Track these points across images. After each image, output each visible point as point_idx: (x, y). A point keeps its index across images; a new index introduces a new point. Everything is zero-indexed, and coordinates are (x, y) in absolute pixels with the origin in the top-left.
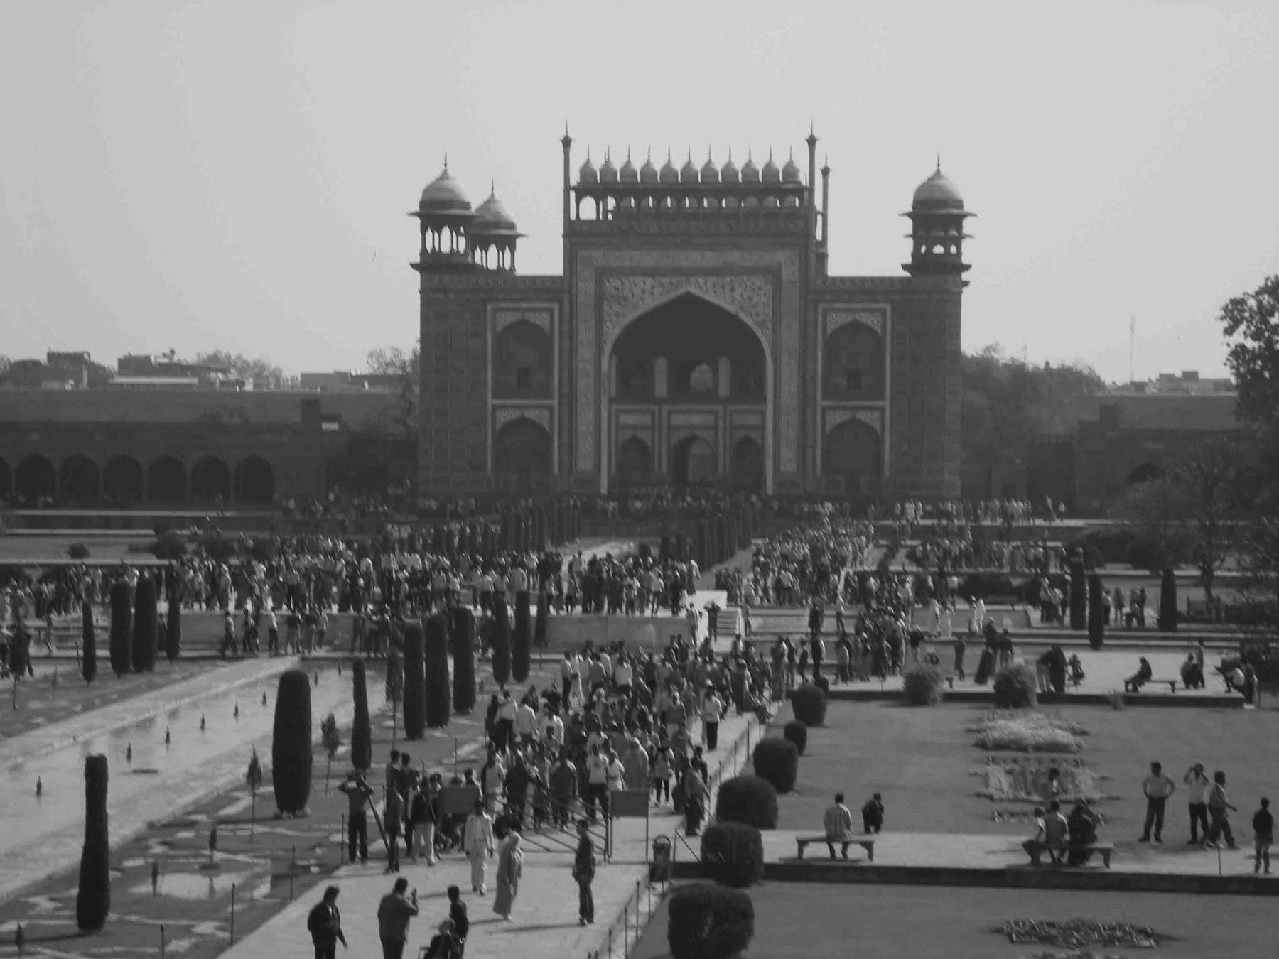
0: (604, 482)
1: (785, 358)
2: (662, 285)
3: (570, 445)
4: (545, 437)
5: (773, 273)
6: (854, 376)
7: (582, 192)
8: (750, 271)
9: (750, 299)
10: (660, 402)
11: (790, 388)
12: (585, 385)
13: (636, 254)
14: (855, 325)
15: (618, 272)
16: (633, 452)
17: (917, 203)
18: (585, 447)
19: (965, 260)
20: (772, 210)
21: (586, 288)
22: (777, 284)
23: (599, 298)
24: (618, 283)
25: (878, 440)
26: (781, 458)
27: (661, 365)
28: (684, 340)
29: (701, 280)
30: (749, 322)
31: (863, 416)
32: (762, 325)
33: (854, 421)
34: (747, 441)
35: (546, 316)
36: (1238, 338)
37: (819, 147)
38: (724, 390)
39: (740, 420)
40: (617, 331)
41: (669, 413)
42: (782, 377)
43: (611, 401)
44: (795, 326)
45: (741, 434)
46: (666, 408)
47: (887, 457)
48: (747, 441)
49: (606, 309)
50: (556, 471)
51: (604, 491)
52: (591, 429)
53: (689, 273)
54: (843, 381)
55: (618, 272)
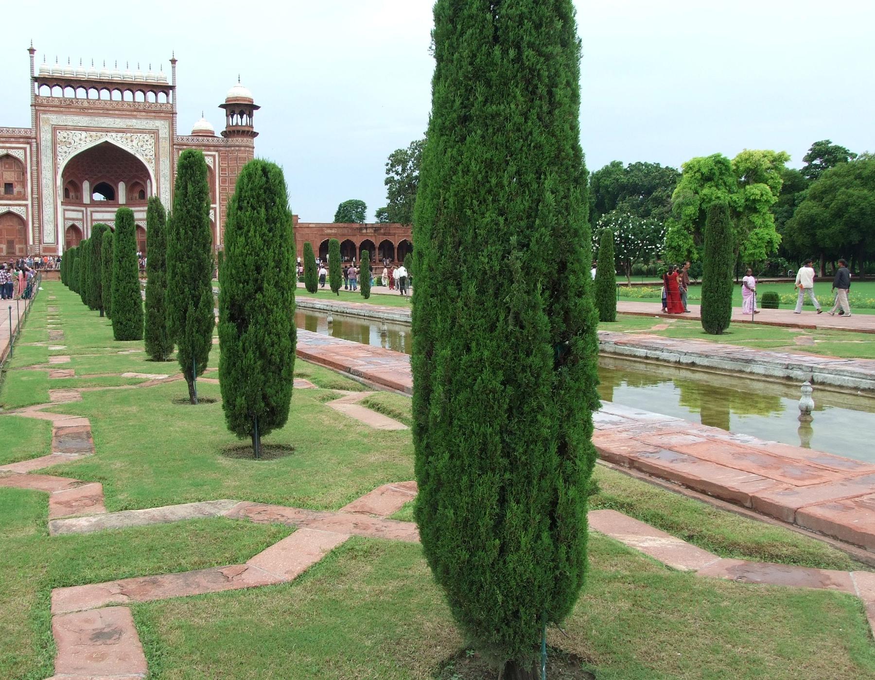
1: (162, 180)
2: (91, 136)
3: (39, 227)
4: (23, 222)
5: (155, 133)
8: (142, 131)
9: (142, 146)
10: (86, 206)
13: (76, 118)
15: (66, 128)
18: (48, 228)
19: (255, 130)
21: (46, 137)
23: (54, 143)
24: (65, 135)
27: (86, 185)
29: (114, 135)
32: (149, 161)
35: (22, 151)
36: (392, 174)
40: (66, 162)
41: (92, 212)
43: (63, 203)
44: (168, 162)
46: (89, 209)
47: (218, 234)
49: (59, 149)
50: (31, 243)
52: (52, 217)
53: (107, 130)
55: (66, 128)
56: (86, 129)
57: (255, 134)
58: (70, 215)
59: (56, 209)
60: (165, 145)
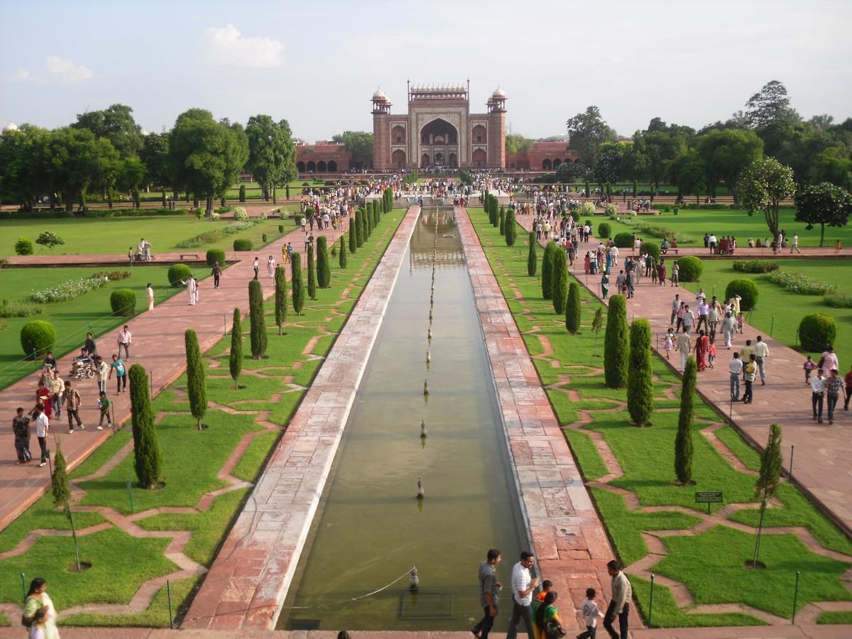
0: (419, 164)
4: (404, 154)
5: (459, 113)
6: (479, 139)
7: (412, 94)
10: (431, 145)
11: (464, 141)
12: (414, 141)
14: (479, 126)
15: (422, 113)
16: (425, 157)
17: (494, 96)
18: (414, 156)
20: (456, 98)
21: (414, 117)
22: (460, 117)
23: (417, 120)
25: (486, 153)
26: (462, 159)
27: (431, 136)
28: (438, 130)
30: (454, 125)
31: (481, 148)
33: (479, 149)
34: (453, 154)
36: (570, 129)
37: (470, 83)
38: (447, 142)
39: (451, 149)
42: (462, 138)
45: (451, 153)
48: (453, 154)
49: (420, 122)
51: (419, 167)
54: (477, 139)
55: (422, 113)
56: (431, 113)
57: (505, 112)
58: (423, 149)
59: (417, 147)
60: (464, 118)
